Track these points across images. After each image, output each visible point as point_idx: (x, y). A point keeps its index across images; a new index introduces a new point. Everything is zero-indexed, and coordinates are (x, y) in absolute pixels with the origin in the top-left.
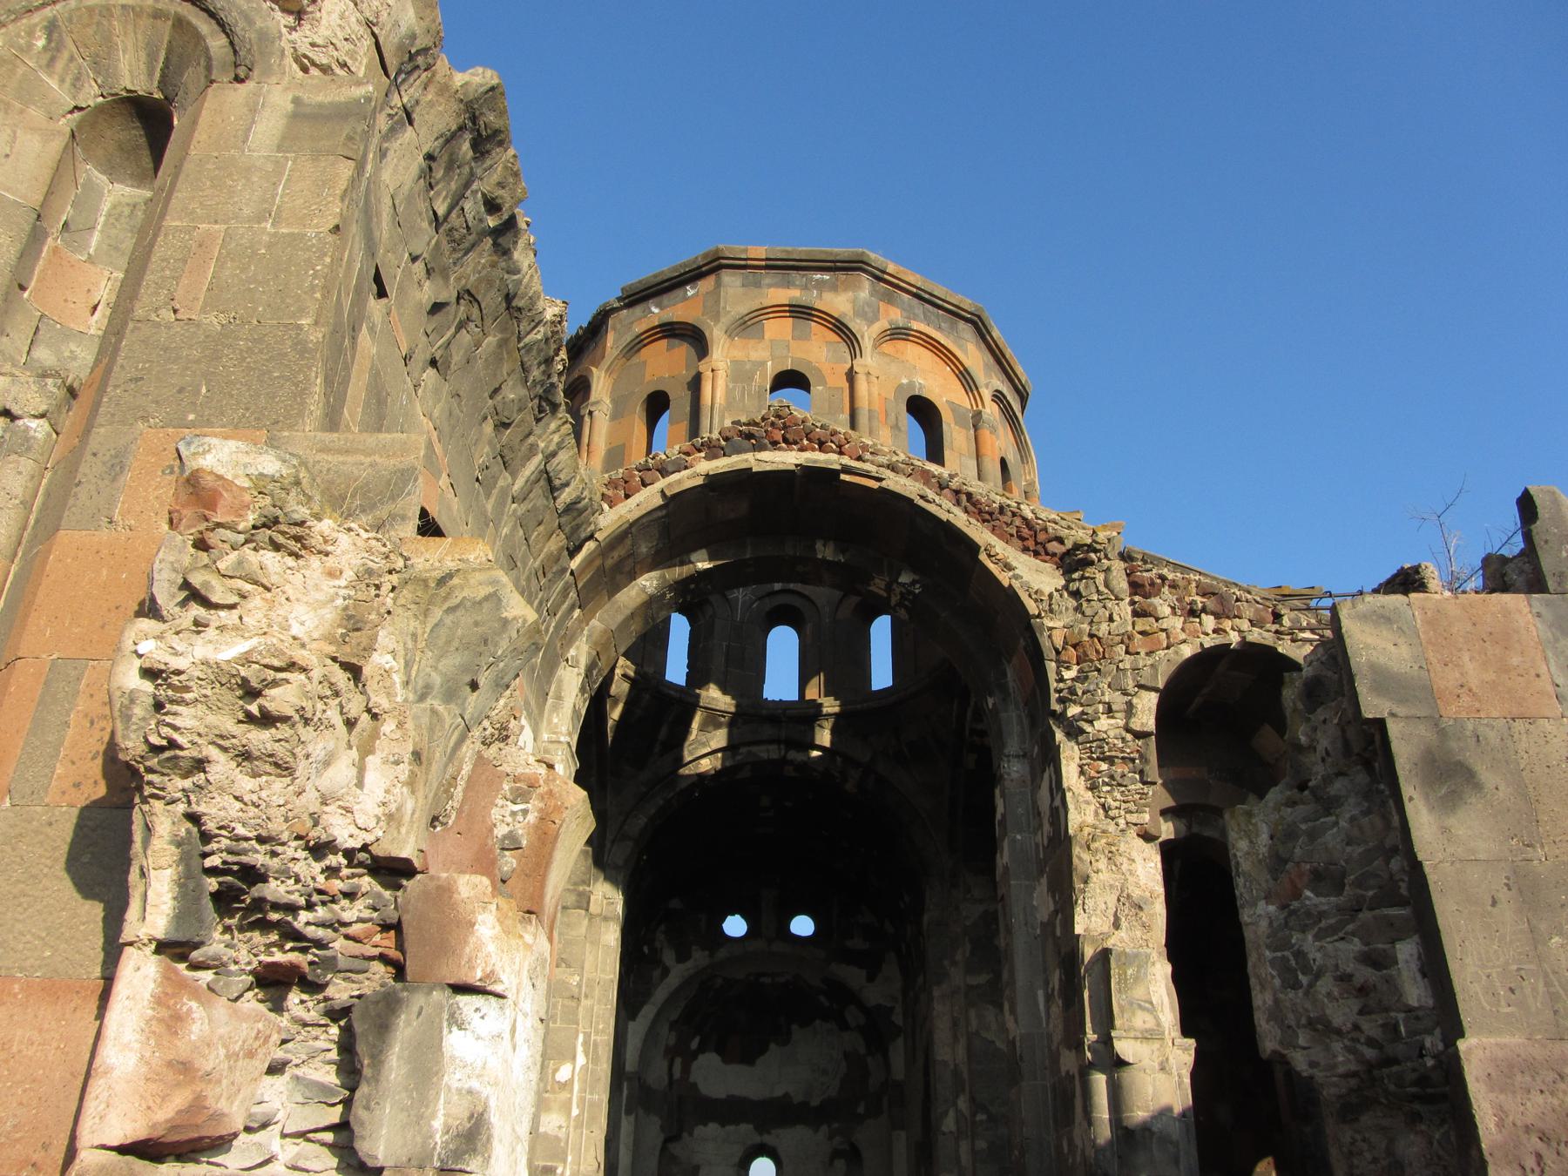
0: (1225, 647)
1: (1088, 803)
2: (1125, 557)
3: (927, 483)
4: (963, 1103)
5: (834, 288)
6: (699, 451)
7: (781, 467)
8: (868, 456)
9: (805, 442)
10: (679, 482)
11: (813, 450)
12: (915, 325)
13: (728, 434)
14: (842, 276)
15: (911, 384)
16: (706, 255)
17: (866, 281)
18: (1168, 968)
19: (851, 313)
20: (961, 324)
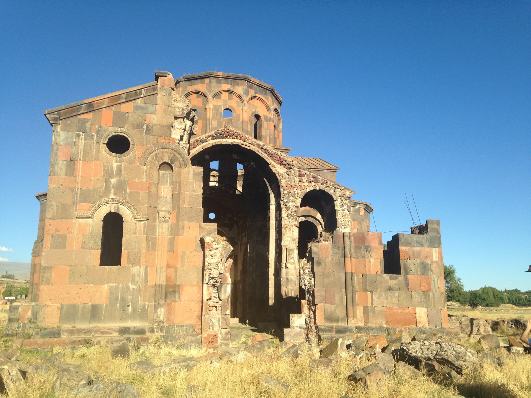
0: (316, 190)
1: (286, 220)
2: (299, 168)
3: (259, 147)
4: (254, 265)
5: (238, 85)
6: (209, 137)
7: (228, 143)
8: (247, 141)
9: (233, 136)
10: (206, 145)
11: (235, 138)
12: (258, 95)
13: (216, 133)
14: (240, 81)
15: (255, 111)
16: (206, 73)
17: (246, 83)
18: (297, 251)
19: (242, 94)
20: (268, 92)
